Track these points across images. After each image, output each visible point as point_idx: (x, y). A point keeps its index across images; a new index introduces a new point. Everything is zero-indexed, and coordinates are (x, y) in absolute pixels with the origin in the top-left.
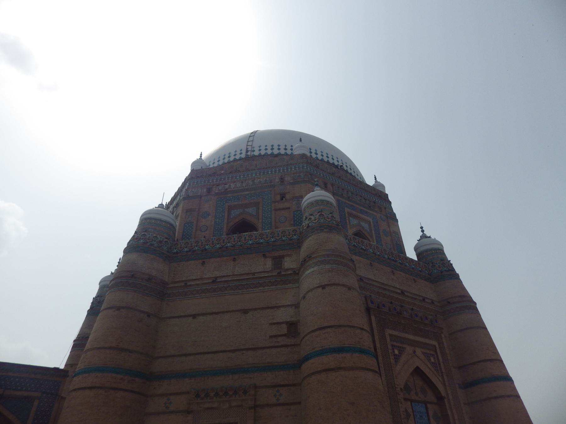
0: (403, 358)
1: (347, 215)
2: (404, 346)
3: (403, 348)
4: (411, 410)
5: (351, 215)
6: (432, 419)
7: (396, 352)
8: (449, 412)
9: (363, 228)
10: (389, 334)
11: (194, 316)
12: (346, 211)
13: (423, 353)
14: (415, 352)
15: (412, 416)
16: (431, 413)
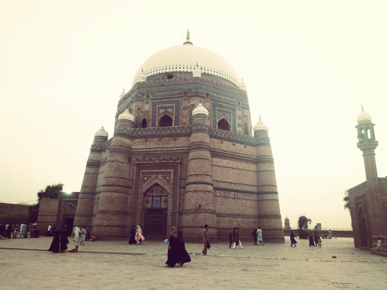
0: (149, 181)
1: (157, 110)
2: (151, 175)
3: (150, 176)
4: (151, 200)
5: (159, 108)
6: (162, 202)
7: (146, 179)
8: (169, 199)
9: (168, 112)
10: (143, 172)
11: (101, 173)
12: (157, 108)
13: (162, 176)
14: (157, 177)
15: (151, 202)
16: (162, 200)
